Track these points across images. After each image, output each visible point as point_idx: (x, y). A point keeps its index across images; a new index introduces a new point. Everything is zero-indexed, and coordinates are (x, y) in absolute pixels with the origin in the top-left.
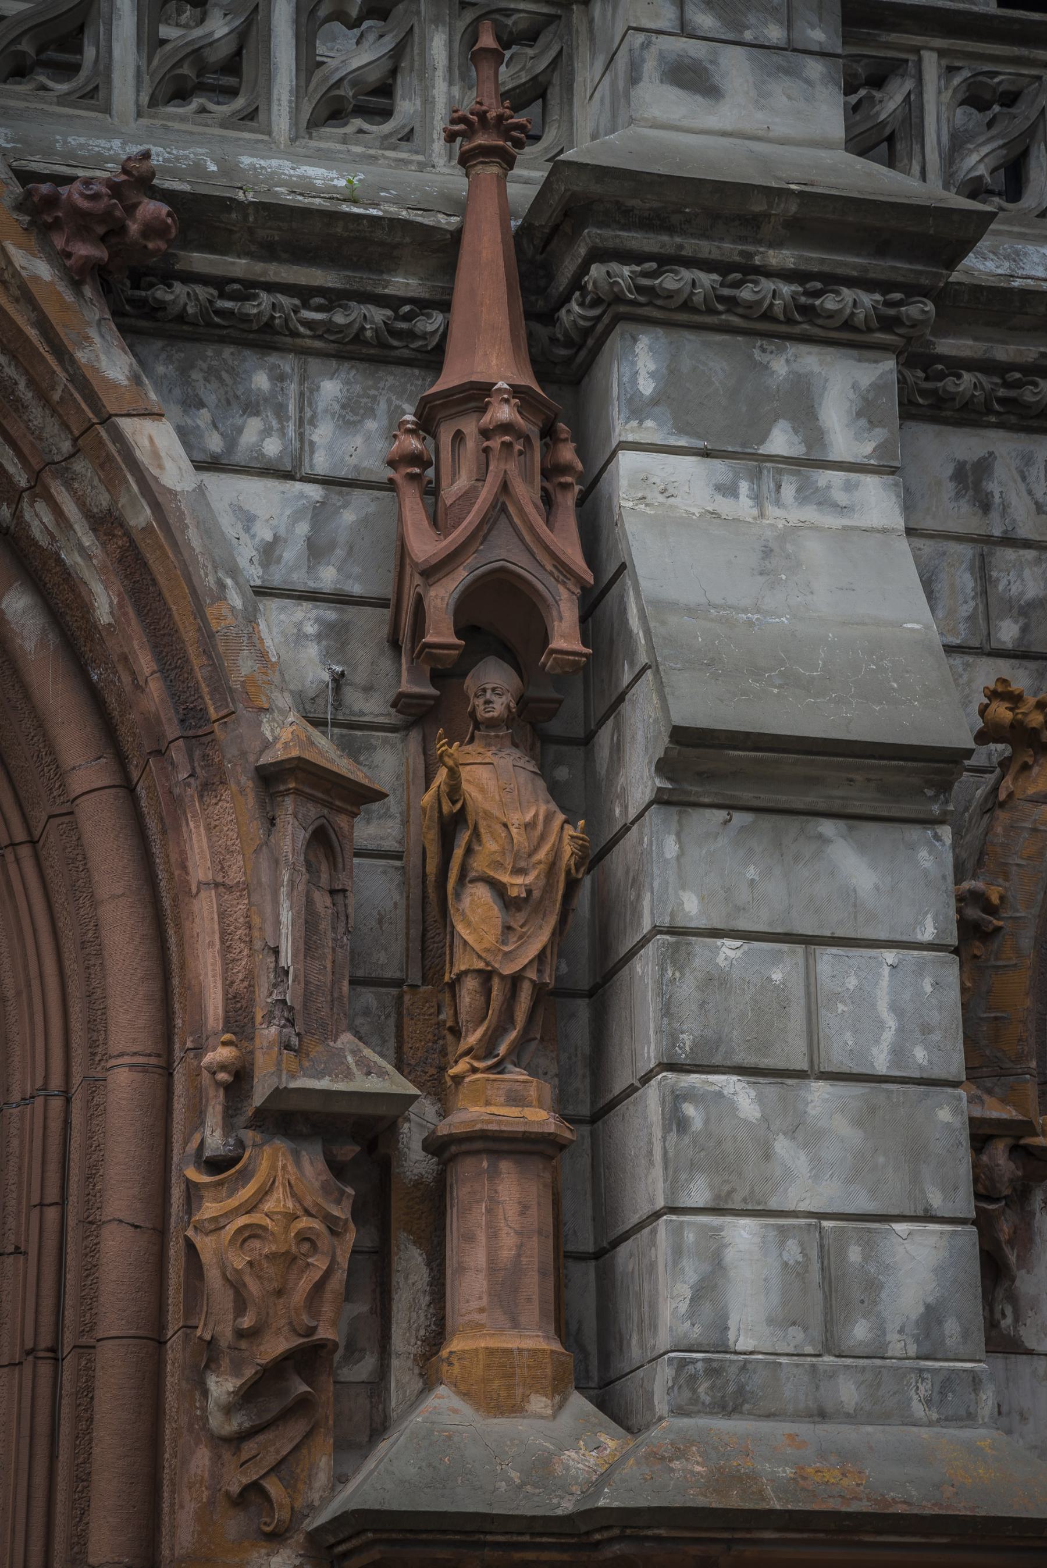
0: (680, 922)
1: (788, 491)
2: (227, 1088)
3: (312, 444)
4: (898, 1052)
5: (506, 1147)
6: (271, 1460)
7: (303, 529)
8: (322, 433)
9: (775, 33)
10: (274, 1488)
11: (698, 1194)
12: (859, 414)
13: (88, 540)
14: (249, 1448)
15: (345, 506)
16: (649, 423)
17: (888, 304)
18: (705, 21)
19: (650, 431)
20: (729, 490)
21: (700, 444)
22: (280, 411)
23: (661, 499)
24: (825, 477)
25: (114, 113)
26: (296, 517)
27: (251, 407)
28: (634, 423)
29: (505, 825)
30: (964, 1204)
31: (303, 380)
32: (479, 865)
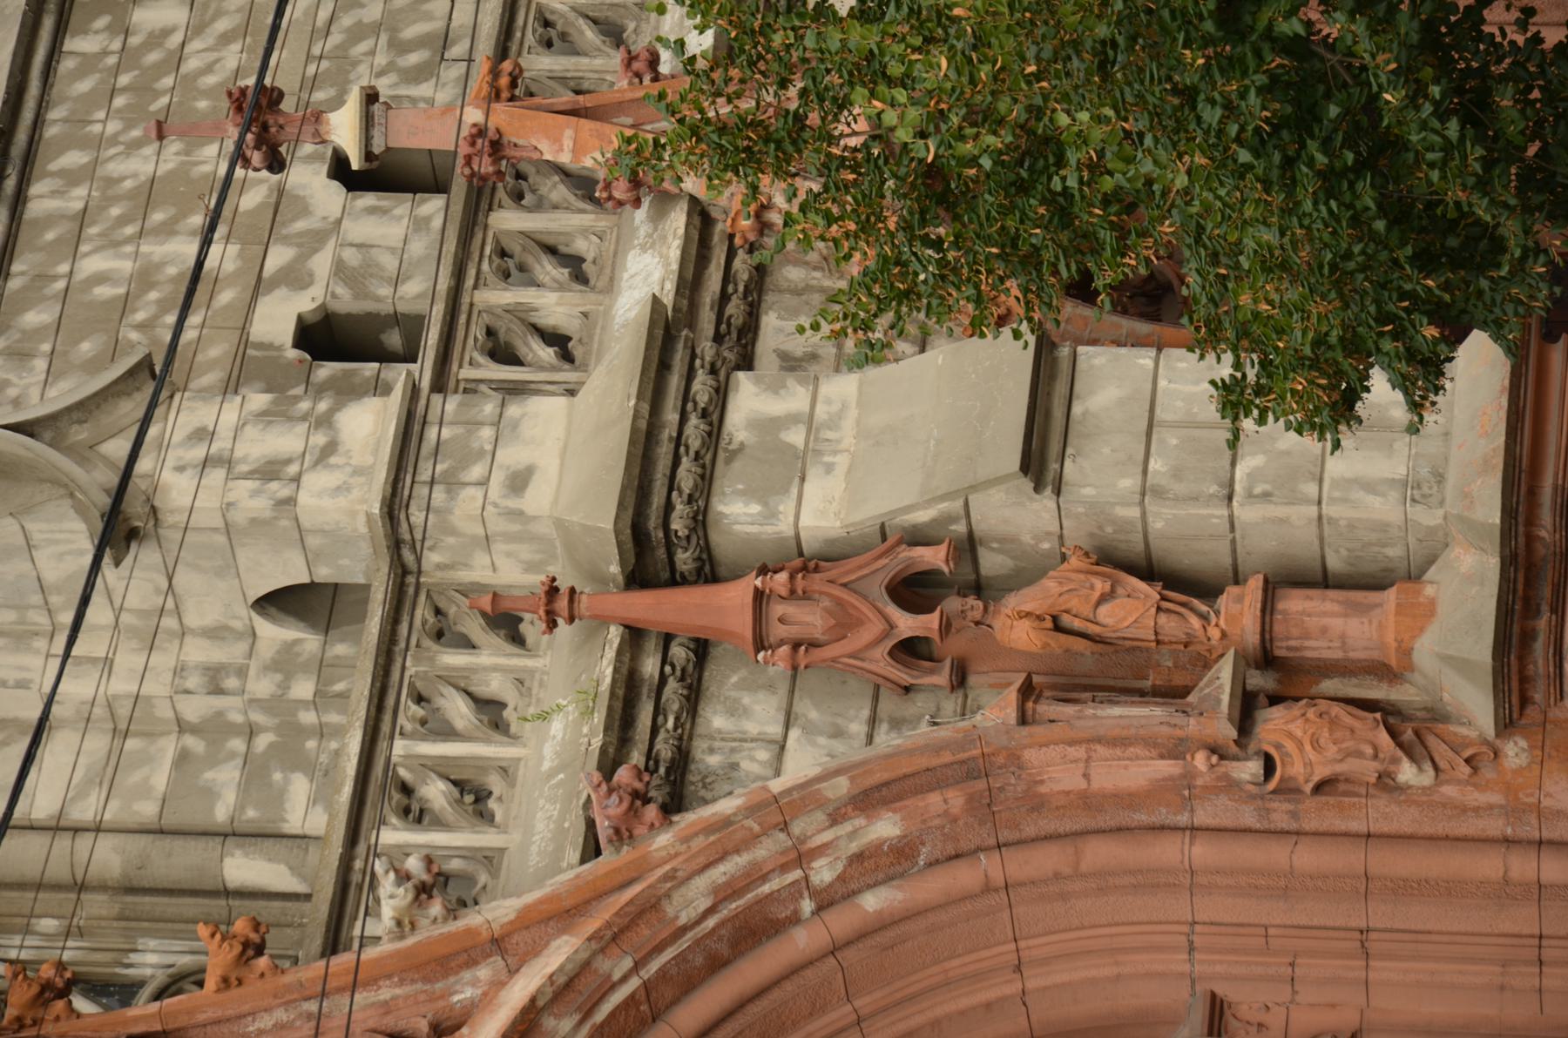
0: (1138, 489)
1: (830, 435)
2: (1222, 757)
3: (759, 734)
5: (1269, 604)
6: (1451, 754)
7: (822, 740)
8: (752, 728)
9: (487, 433)
10: (1468, 753)
11: (1311, 489)
12: (776, 393)
13: (847, 827)
14: (1442, 764)
15: (805, 715)
16: (781, 508)
17: (703, 367)
18: (477, 471)
19: (786, 507)
21: (797, 480)
22: (733, 750)
23: (835, 504)
24: (821, 411)
25: (504, 846)
26: (814, 744)
28: (781, 516)
29: (1060, 595)
31: (712, 738)
32: (1086, 611)
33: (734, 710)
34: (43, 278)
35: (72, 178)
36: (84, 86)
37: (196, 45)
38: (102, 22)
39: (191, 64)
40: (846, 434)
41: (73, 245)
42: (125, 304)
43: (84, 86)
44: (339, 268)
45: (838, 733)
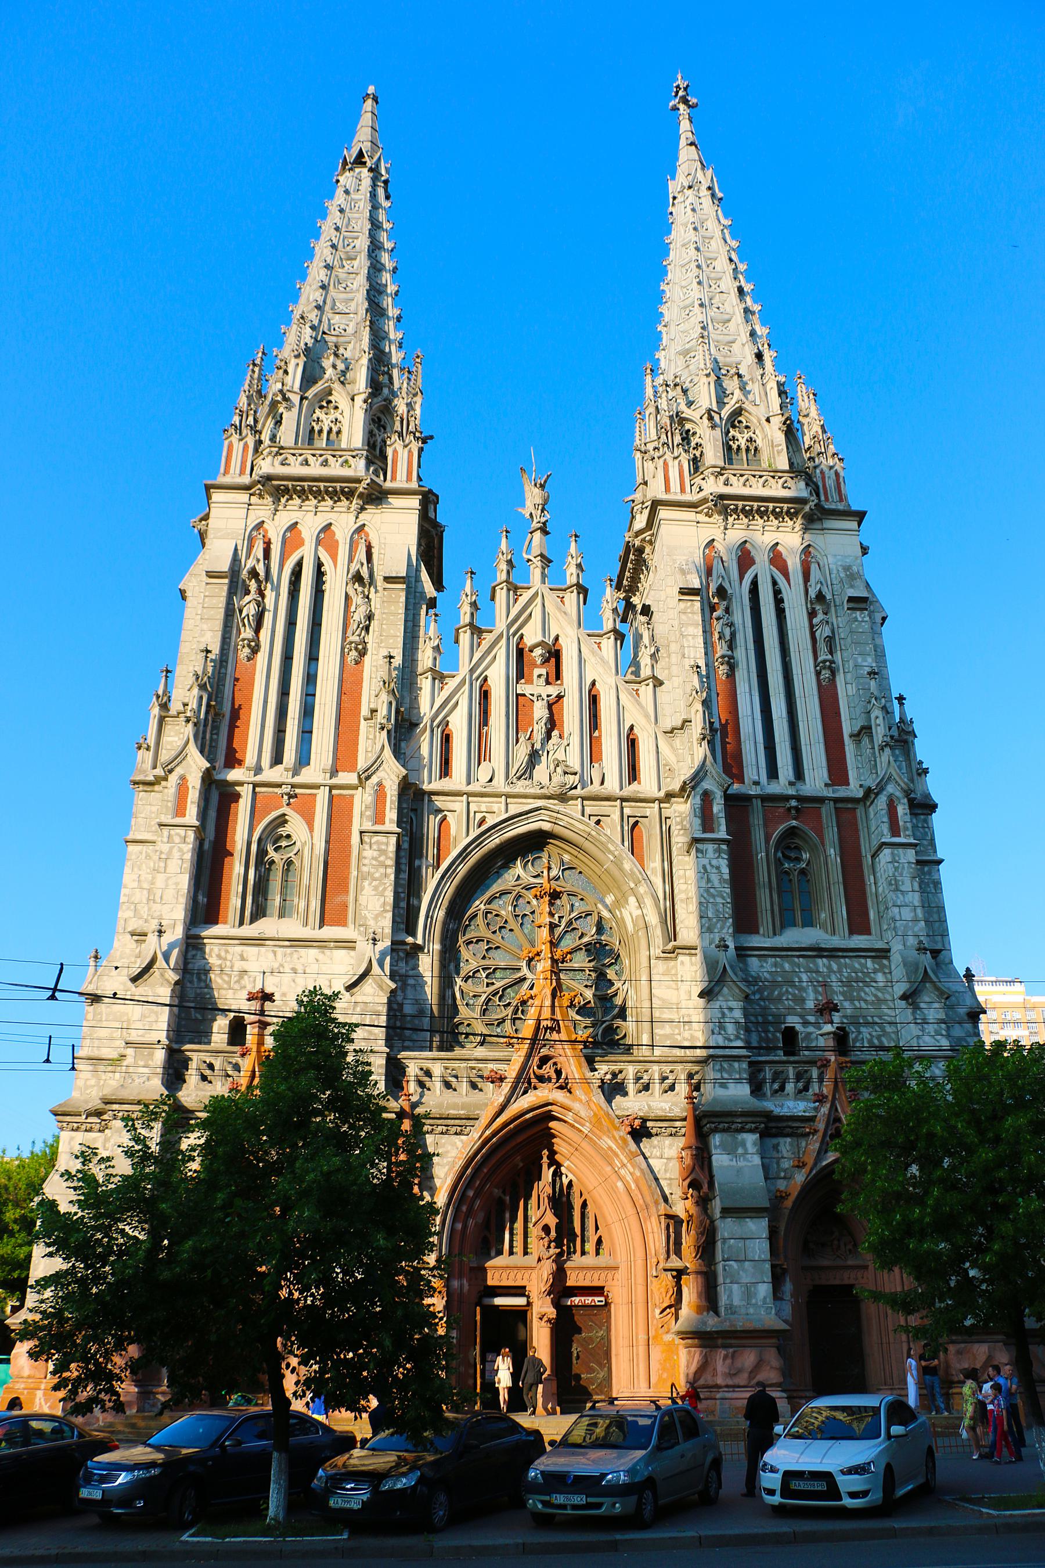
4: (759, 1256)
8: (666, 1150)
9: (737, 1076)
18: (726, 1076)
19: (718, 1151)
20: (732, 1160)
27: (654, 1147)
30: (770, 1280)
33: (671, 1146)
34: (799, 966)
35: (829, 968)
36: (857, 965)
37: (873, 989)
38: (876, 966)
39: (867, 989)
40: (742, 1163)
41: (809, 971)
42: (793, 986)
43: (857, 965)
44: (811, 1033)
45: (666, 1171)
